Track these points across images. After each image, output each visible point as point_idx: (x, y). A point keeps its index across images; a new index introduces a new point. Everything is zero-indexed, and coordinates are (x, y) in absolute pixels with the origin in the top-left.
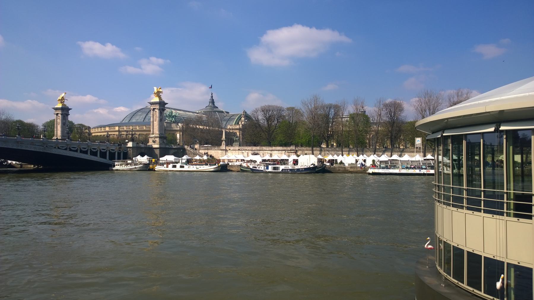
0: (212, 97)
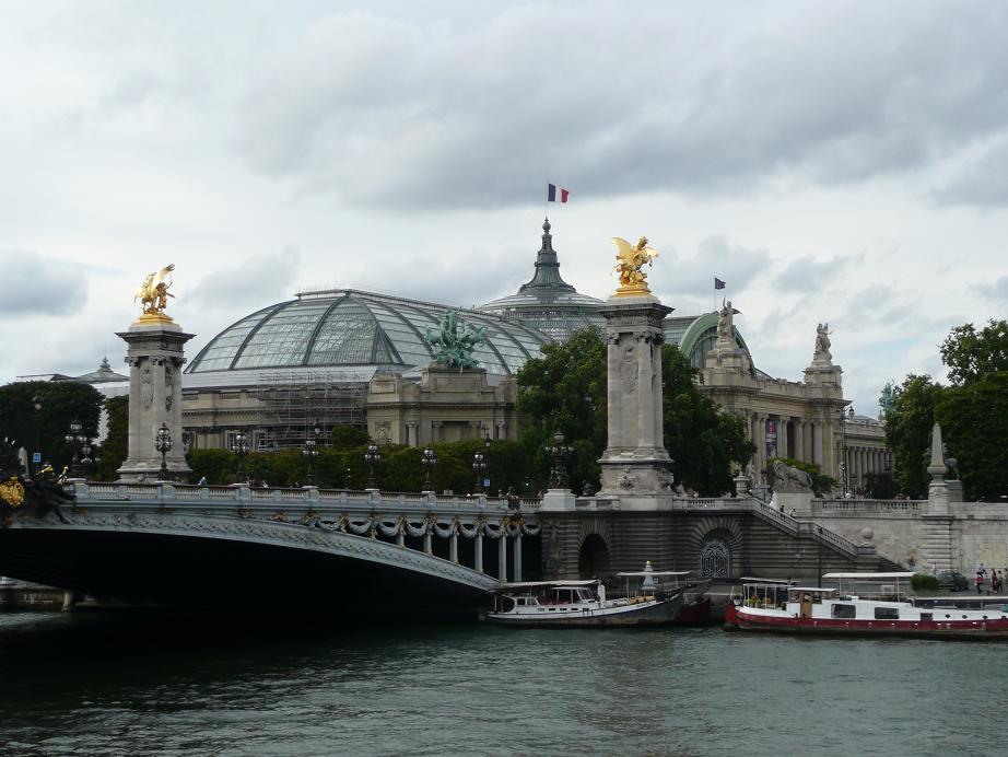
0: (547, 240)
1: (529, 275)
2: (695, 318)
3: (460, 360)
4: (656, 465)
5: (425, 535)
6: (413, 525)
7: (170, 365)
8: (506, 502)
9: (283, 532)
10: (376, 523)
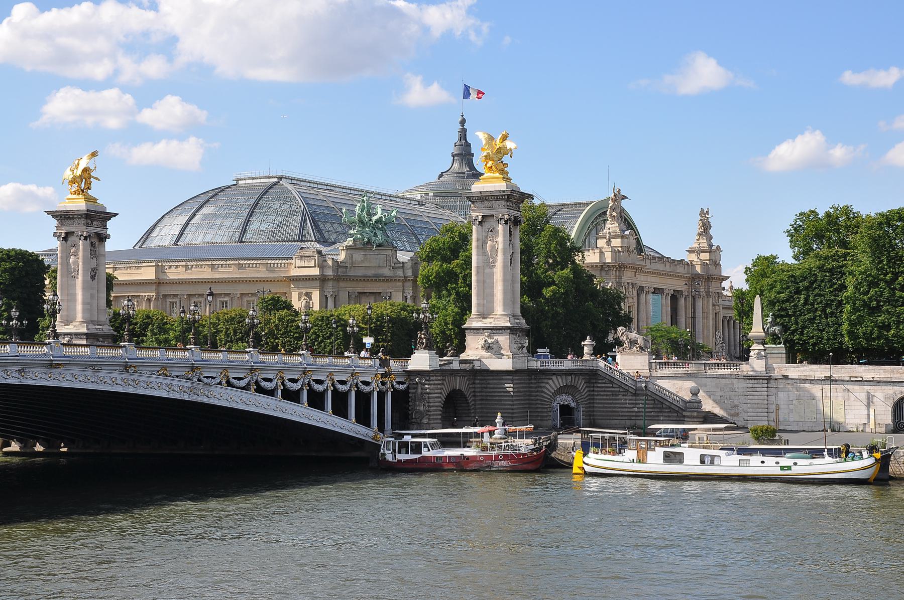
0: (463, 133)
2: (588, 204)
3: (374, 239)
4: (512, 330)
5: (301, 389)
6: (290, 380)
7: (95, 240)
8: (378, 362)
9: (168, 385)
10: (255, 378)
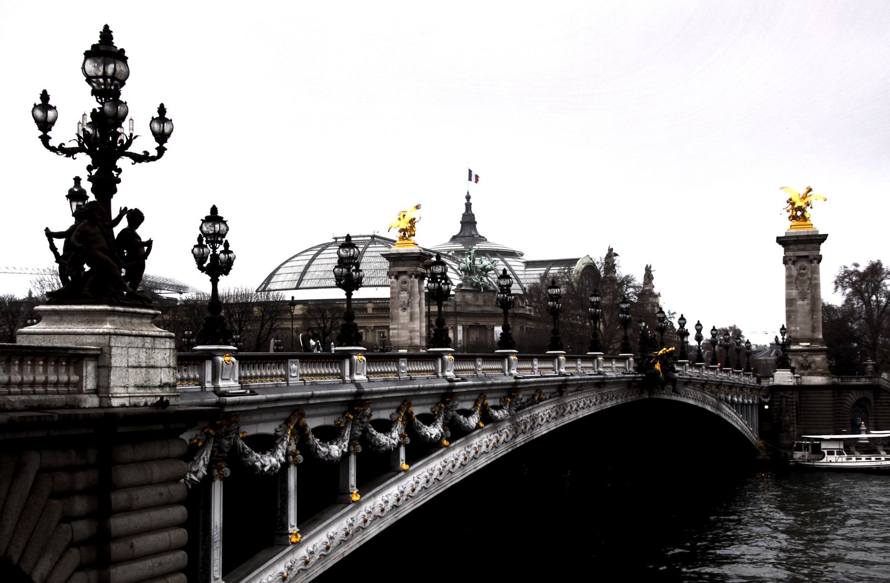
0: (468, 206)
1: (456, 229)
